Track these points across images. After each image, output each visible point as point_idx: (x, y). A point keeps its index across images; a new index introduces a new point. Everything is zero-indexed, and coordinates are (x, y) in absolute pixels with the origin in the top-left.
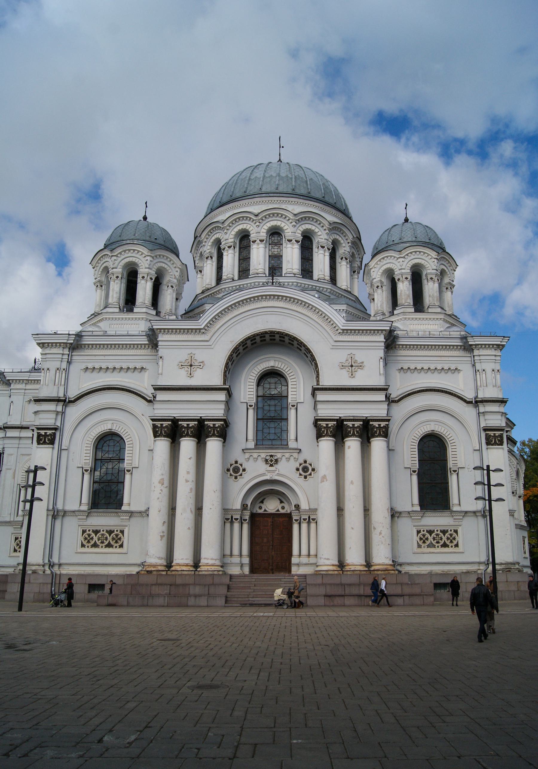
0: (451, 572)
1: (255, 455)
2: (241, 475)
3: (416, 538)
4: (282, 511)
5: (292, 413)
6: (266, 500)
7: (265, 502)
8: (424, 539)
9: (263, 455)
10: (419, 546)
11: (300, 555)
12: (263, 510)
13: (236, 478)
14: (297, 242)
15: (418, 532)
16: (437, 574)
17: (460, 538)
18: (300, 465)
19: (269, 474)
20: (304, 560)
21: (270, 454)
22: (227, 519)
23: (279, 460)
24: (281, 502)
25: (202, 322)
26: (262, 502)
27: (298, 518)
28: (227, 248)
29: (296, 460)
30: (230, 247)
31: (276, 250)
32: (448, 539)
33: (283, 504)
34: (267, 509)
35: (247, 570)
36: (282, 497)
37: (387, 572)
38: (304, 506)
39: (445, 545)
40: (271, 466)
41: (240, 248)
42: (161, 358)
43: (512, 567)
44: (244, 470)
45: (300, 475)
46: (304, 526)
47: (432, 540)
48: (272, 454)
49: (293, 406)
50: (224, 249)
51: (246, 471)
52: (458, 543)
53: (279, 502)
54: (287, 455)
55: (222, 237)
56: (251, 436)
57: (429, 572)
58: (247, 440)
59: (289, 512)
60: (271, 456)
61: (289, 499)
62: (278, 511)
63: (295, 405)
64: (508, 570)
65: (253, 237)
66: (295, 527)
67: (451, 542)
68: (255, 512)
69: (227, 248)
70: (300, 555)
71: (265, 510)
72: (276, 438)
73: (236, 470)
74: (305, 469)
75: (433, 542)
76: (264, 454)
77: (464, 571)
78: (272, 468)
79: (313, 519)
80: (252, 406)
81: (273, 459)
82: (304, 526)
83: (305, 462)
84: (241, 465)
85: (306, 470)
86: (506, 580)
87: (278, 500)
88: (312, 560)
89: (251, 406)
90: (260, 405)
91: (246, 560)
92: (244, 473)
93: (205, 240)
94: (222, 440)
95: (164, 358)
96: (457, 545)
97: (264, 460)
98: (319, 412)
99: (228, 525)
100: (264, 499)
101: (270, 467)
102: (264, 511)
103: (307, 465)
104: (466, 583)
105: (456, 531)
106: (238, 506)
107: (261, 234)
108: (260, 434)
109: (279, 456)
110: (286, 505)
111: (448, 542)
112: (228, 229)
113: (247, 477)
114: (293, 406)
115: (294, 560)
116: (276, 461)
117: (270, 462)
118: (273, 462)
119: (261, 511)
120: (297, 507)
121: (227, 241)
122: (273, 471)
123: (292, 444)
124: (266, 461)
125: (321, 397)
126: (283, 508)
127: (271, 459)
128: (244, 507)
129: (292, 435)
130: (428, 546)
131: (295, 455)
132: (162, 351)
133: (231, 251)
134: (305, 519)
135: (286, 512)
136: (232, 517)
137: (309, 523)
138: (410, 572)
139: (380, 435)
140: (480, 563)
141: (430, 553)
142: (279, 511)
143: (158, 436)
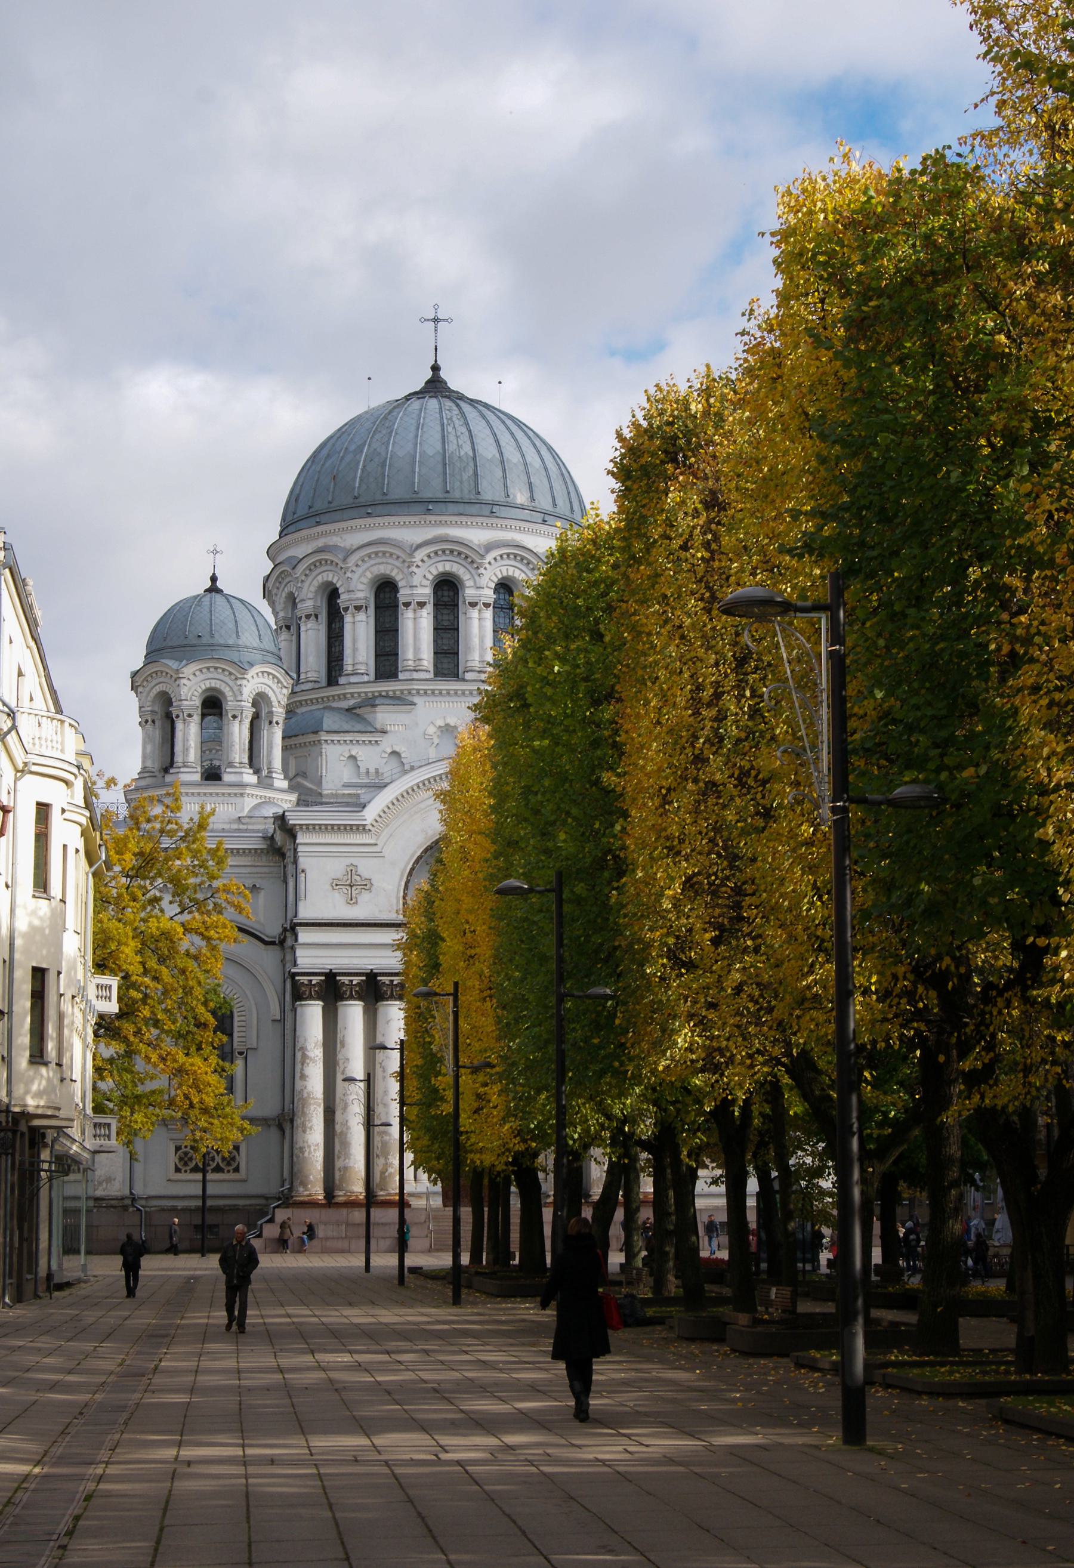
14: (487, 605)
25: (370, 814)
28: (352, 609)
30: (358, 608)
31: (446, 617)
41: (377, 608)
42: (303, 871)
50: (346, 609)
65: (403, 595)
69: (352, 609)
93: (303, 578)
95: (307, 871)
107: (420, 591)
121: (352, 596)
132: (303, 862)
133: (361, 616)
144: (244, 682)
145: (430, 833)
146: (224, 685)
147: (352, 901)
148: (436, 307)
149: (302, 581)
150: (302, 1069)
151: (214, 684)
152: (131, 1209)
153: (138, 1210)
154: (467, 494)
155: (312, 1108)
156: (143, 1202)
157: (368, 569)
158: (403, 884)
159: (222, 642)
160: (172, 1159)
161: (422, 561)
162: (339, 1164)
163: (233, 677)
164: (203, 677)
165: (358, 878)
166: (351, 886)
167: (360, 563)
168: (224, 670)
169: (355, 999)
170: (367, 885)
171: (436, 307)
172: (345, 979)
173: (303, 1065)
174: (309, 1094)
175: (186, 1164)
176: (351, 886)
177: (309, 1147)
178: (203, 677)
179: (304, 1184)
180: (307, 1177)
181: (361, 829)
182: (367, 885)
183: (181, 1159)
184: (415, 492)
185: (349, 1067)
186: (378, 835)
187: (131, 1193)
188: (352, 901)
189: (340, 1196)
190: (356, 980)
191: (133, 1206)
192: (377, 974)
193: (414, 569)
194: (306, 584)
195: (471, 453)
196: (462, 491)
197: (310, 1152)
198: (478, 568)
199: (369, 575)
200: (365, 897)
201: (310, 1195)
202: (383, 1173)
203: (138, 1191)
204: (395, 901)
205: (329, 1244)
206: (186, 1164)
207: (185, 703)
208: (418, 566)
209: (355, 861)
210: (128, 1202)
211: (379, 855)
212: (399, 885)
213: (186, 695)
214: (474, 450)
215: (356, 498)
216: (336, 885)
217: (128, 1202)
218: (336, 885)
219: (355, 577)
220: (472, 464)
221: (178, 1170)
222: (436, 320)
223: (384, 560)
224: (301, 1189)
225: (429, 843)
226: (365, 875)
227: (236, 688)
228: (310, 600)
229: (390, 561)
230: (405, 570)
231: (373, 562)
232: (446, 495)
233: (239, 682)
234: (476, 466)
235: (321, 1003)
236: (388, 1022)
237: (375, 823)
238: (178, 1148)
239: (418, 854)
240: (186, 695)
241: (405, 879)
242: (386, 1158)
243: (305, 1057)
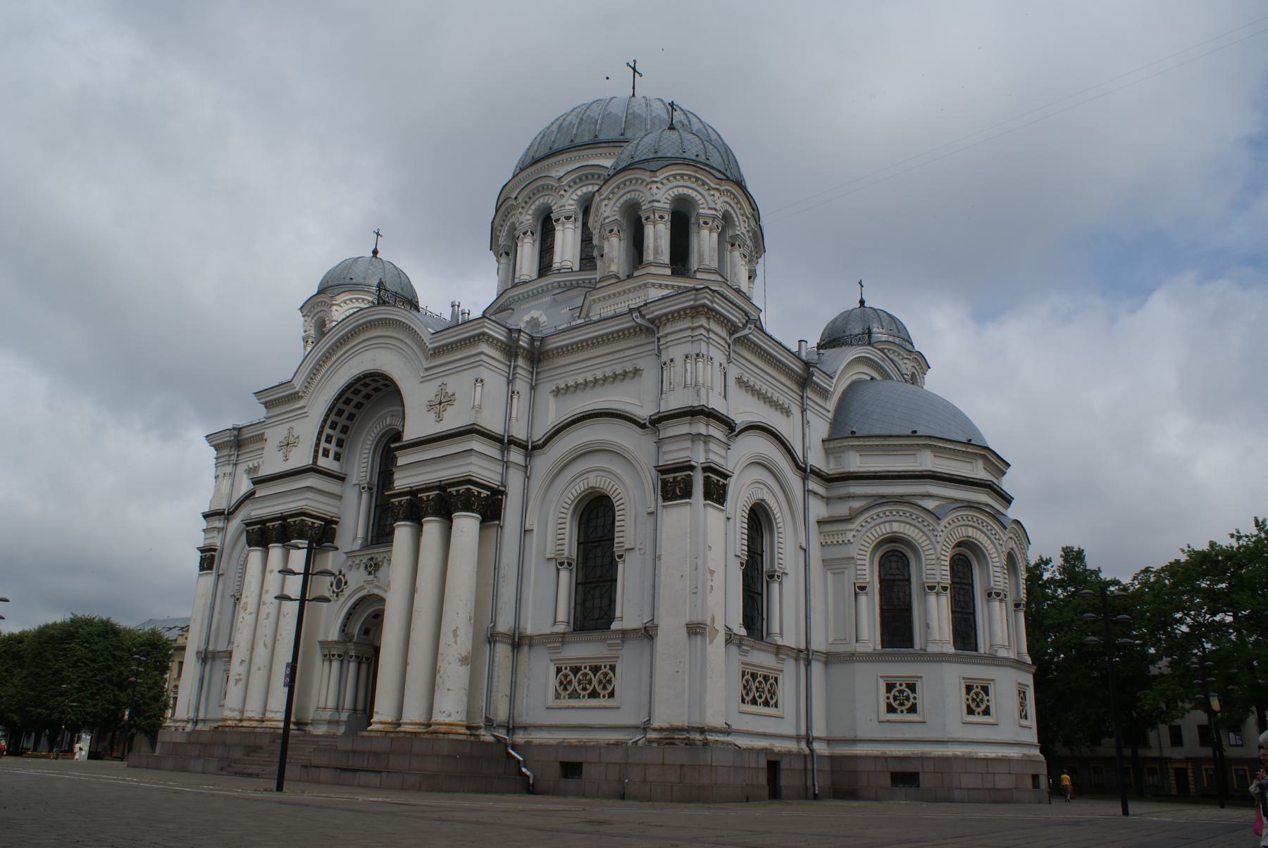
0: (592, 743)
3: (552, 681)
8: (564, 684)
10: (558, 696)
15: (559, 670)
16: (571, 747)
17: (617, 683)
30: (568, 218)
32: (600, 682)
37: (434, 735)
39: (594, 694)
43: (676, 737)
47: (576, 684)
52: (613, 689)
55: (554, 202)
57: (559, 743)
64: (668, 741)
67: (605, 688)
75: (577, 688)
77: (612, 742)
86: (661, 762)
96: (612, 695)
104: (607, 763)
105: (613, 668)
111: (599, 689)
130: (571, 696)
138: (532, 740)
140: (636, 728)
141: (568, 708)
228: (526, 218)
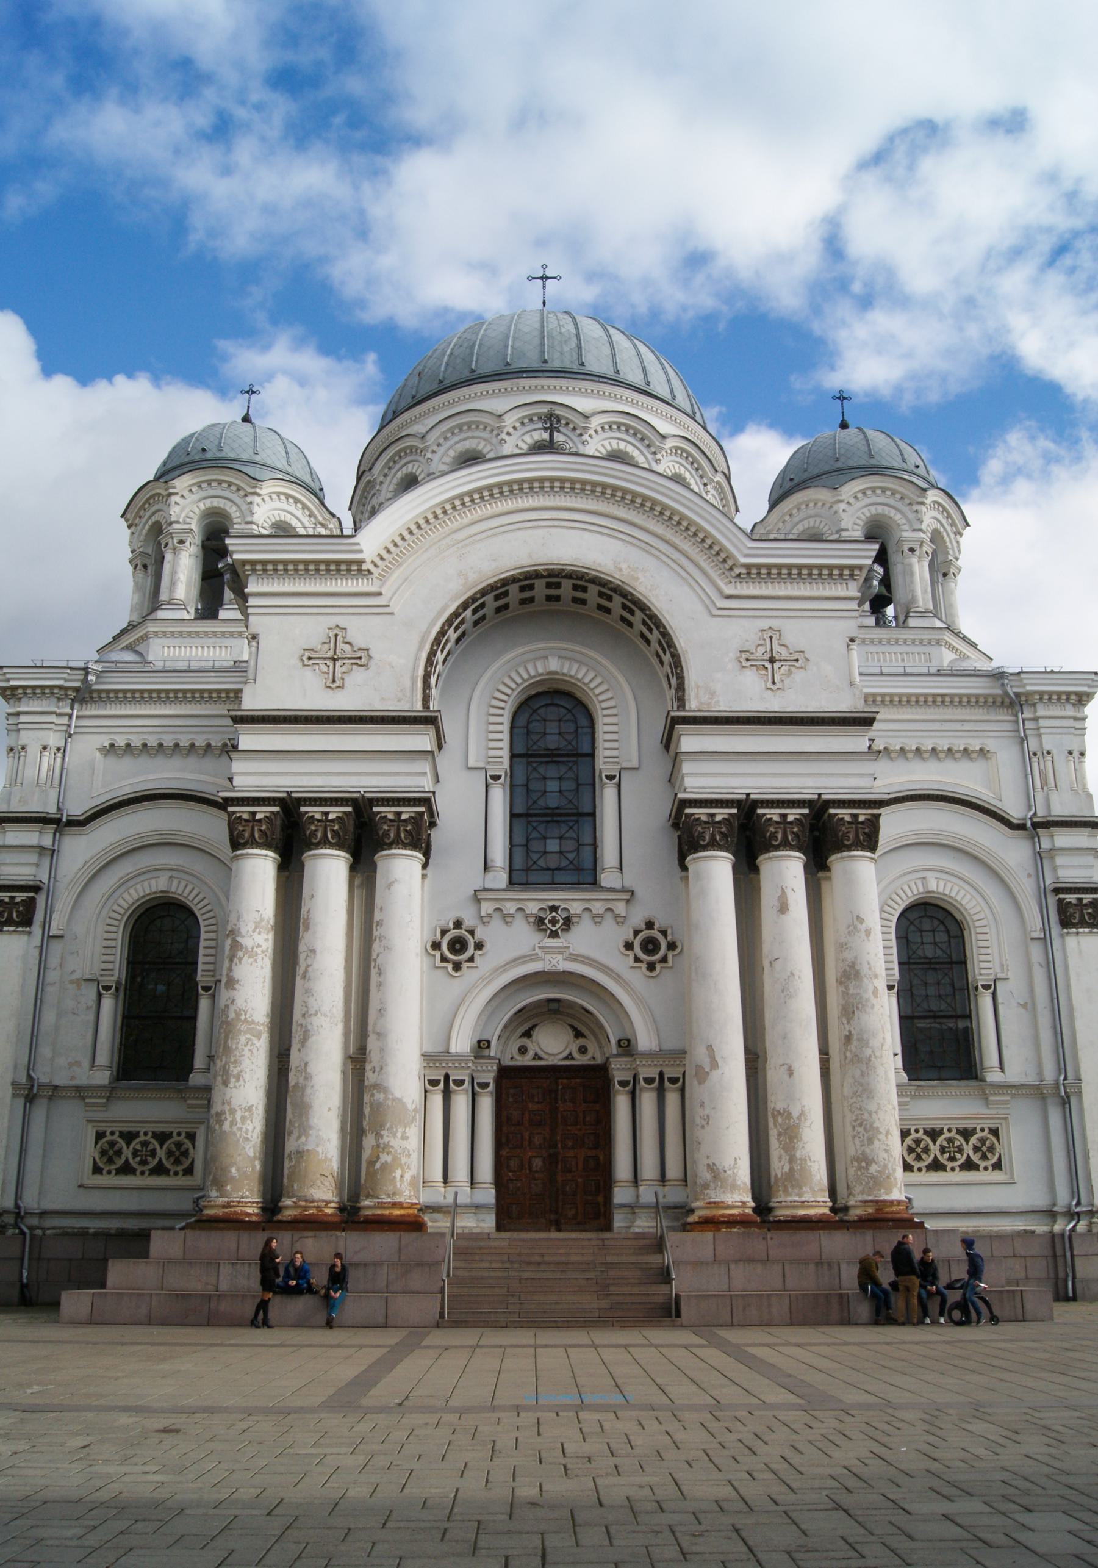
1: (510, 908)
2: (471, 959)
4: (581, 1060)
5: (608, 796)
6: (537, 1029)
7: (535, 1033)
9: (533, 908)
11: (636, 1180)
12: (531, 1054)
13: (457, 967)
18: (636, 933)
19: (548, 957)
20: (647, 1195)
21: (551, 904)
22: (434, 1083)
23: (574, 920)
24: (578, 1034)
26: (528, 1034)
27: (627, 1076)
29: (619, 920)
33: (581, 1041)
34: (540, 1053)
35: (488, 1222)
36: (580, 1020)
38: (645, 1041)
40: (554, 935)
44: (479, 946)
45: (637, 959)
46: (647, 1101)
48: (557, 904)
49: (611, 778)
51: (484, 950)
53: (571, 1033)
54: (598, 907)
56: (499, 854)
58: (486, 868)
59: (599, 1061)
60: (554, 909)
61: (602, 1027)
62: (570, 1057)
63: (613, 777)
66: (621, 1104)
68: (507, 1062)
70: (636, 1180)
71: (537, 1057)
72: (564, 863)
73: (458, 945)
74: (649, 946)
76: (535, 902)
78: (556, 940)
79: (673, 1081)
80: (498, 777)
81: (558, 918)
82: (647, 1101)
83: (650, 925)
84: (472, 933)
85: (650, 947)
87: (570, 1030)
88: (673, 1195)
89: (496, 778)
90: (520, 779)
91: (488, 1195)
92: (478, 952)
94: (420, 856)
97: (532, 919)
98: (689, 782)
99: (437, 1100)
100: (534, 1026)
101: (551, 940)
102: (534, 1059)
103: (655, 933)
106: (461, 1043)
108: (519, 853)
109: (575, 908)
110: (593, 1049)
112: (433, 452)
113: (485, 962)
114: (611, 778)
115: (621, 1195)
116: (568, 922)
117: (550, 926)
118: (558, 926)
119: (526, 1060)
120: (626, 1046)
122: (560, 950)
123: (607, 879)
124: (540, 921)
125: (690, 741)
126: (583, 1050)
127: (554, 917)
128: (482, 1045)
129: (609, 854)
131: (620, 908)
134: (649, 1081)
135: (592, 1063)
136: (447, 1077)
137: (661, 1093)
139: (858, 845)
142: (573, 1058)
143: (244, 846)
144: (257, 499)
145: (472, 577)
146: (229, 504)
147: (334, 684)
148: (544, 267)
149: (382, 483)
150: (230, 969)
151: (216, 503)
152: (10, 1232)
153: (23, 1233)
154: (570, 364)
155: (243, 1039)
156: (34, 1221)
157: (451, 447)
158: (424, 656)
159: (232, 455)
160: (90, 1151)
161: (514, 428)
162: (291, 1145)
163: (242, 493)
164: (203, 494)
165: (347, 647)
166: (334, 660)
167: (441, 441)
168: (230, 484)
169: (332, 846)
170: (360, 658)
171: (544, 267)
172: (316, 811)
173: (231, 960)
174: (238, 1014)
175: (110, 1161)
176: (334, 660)
177: (233, 1112)
178: (203, 494)
179: (219, 1184)
180: (225, 1170)
181: (353, 568)
182: (360, 658)
183: (103, 1153)
184: (508, 364)
185: (315, 966)
186: (382, 578)
187: (17, 1206)
188: (334, 684)
189: (289, 1208)
190: (335, 812)
191: (16, 1225)
192: (373, 802)
193: (504, 436)
194: (385, 486)
195: (574, 331)
196: (562, 361)
197: (233, 1123)
198: (581, 435)
199: (452, 453)
200: (357, 676)
201: (228, 1205)
202: (371, 1163)
203: (30, 1201)
204: (408, 683)
205: (224, 1306)
206: (110, 1161)
207: (176, 526)
208: (508, 434)
209: (342, 621)
210: (10, 1219)
211: (385, 610)
212: (417, 658)
213: (178, 516)
214: (577, 329)
215: (441, 382)
216: (309, 657)
217: (10, 1219)
218: (309, 657)
219: (436, 458)
220: (575, 339)
221: (97, 1170)
222: (544, 278)
223: (470, 434)
224: (214, 1193)
225: (470, 593)
226: (360, 641)
227: (244, 507)
229: (477, 433)
230: (494, 441)
231: (456, 439)
232: (544, 365)
233: (249, 499)
234: (579, 340)
235: (271, 854)
236: (389, 886)
237: (378, 560)
238: (100, 1136)
239: (452, 609)
240: (178, 516)
241: (427, 649)
242: (379, 1136)
243: (236, 946)
